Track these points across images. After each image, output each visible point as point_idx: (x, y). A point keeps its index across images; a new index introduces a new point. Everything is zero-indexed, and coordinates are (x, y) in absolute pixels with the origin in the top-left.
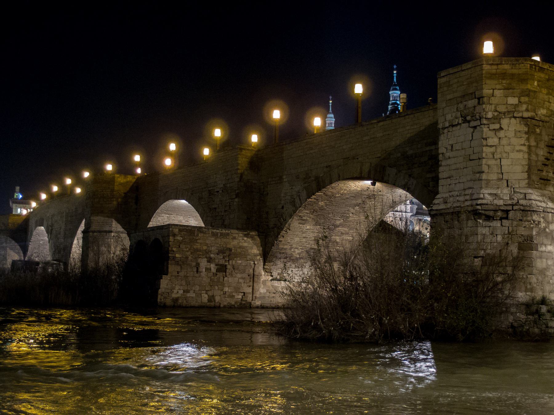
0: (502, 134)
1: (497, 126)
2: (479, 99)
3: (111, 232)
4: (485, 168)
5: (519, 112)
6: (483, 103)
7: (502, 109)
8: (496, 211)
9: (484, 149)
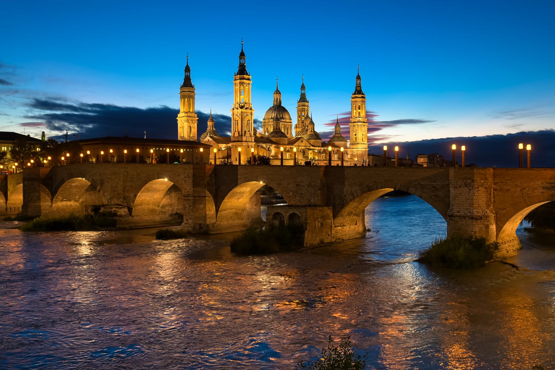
0: (479, 192)
1: (478, 190)
2: (472, 181)
3: (206, 197)
4: (474, 203)
5: (484, 185)
6: (474, 182)
7: (479, 184)
8: (478, 217)
9: (474, 197)
